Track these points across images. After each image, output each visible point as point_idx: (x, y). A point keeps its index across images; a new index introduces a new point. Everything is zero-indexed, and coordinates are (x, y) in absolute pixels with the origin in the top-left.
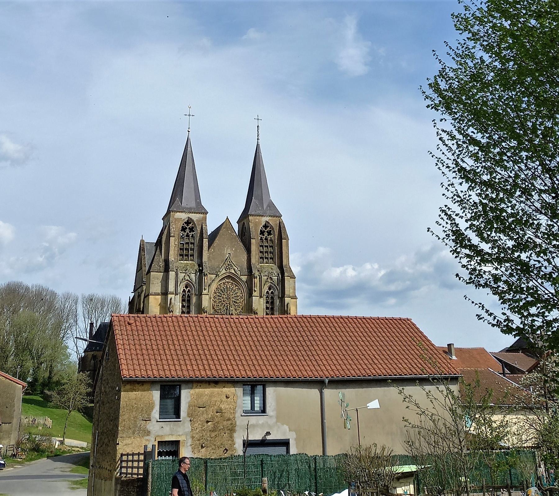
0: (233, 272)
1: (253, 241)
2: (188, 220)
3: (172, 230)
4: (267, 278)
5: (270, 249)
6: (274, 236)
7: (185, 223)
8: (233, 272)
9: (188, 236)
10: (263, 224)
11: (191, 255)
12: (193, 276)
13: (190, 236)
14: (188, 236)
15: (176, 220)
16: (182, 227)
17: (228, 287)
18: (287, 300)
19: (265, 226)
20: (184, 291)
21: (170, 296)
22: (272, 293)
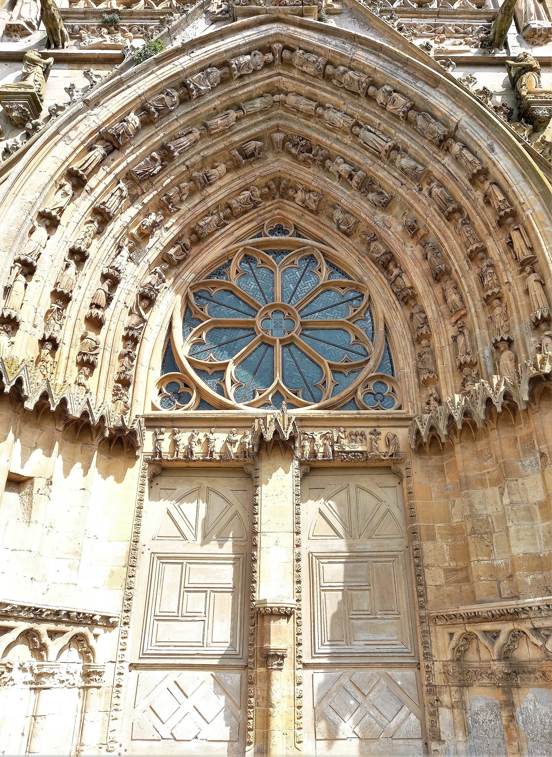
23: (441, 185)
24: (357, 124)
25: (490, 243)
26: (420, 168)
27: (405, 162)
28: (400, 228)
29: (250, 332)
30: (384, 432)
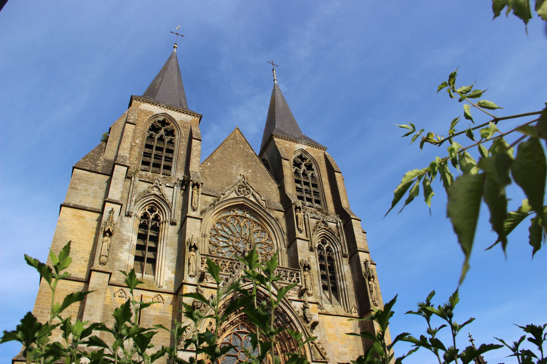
0: (252, 199)
1: (285, 162)
4: (317, 223)
7: (159, 122)
8: (252, 199)
15: (141, 111)
18: (363, 257)
19: (300, 157)
20: (145, 216)
22: (328, 249)
27: (280, 322)
29: (235, 358)
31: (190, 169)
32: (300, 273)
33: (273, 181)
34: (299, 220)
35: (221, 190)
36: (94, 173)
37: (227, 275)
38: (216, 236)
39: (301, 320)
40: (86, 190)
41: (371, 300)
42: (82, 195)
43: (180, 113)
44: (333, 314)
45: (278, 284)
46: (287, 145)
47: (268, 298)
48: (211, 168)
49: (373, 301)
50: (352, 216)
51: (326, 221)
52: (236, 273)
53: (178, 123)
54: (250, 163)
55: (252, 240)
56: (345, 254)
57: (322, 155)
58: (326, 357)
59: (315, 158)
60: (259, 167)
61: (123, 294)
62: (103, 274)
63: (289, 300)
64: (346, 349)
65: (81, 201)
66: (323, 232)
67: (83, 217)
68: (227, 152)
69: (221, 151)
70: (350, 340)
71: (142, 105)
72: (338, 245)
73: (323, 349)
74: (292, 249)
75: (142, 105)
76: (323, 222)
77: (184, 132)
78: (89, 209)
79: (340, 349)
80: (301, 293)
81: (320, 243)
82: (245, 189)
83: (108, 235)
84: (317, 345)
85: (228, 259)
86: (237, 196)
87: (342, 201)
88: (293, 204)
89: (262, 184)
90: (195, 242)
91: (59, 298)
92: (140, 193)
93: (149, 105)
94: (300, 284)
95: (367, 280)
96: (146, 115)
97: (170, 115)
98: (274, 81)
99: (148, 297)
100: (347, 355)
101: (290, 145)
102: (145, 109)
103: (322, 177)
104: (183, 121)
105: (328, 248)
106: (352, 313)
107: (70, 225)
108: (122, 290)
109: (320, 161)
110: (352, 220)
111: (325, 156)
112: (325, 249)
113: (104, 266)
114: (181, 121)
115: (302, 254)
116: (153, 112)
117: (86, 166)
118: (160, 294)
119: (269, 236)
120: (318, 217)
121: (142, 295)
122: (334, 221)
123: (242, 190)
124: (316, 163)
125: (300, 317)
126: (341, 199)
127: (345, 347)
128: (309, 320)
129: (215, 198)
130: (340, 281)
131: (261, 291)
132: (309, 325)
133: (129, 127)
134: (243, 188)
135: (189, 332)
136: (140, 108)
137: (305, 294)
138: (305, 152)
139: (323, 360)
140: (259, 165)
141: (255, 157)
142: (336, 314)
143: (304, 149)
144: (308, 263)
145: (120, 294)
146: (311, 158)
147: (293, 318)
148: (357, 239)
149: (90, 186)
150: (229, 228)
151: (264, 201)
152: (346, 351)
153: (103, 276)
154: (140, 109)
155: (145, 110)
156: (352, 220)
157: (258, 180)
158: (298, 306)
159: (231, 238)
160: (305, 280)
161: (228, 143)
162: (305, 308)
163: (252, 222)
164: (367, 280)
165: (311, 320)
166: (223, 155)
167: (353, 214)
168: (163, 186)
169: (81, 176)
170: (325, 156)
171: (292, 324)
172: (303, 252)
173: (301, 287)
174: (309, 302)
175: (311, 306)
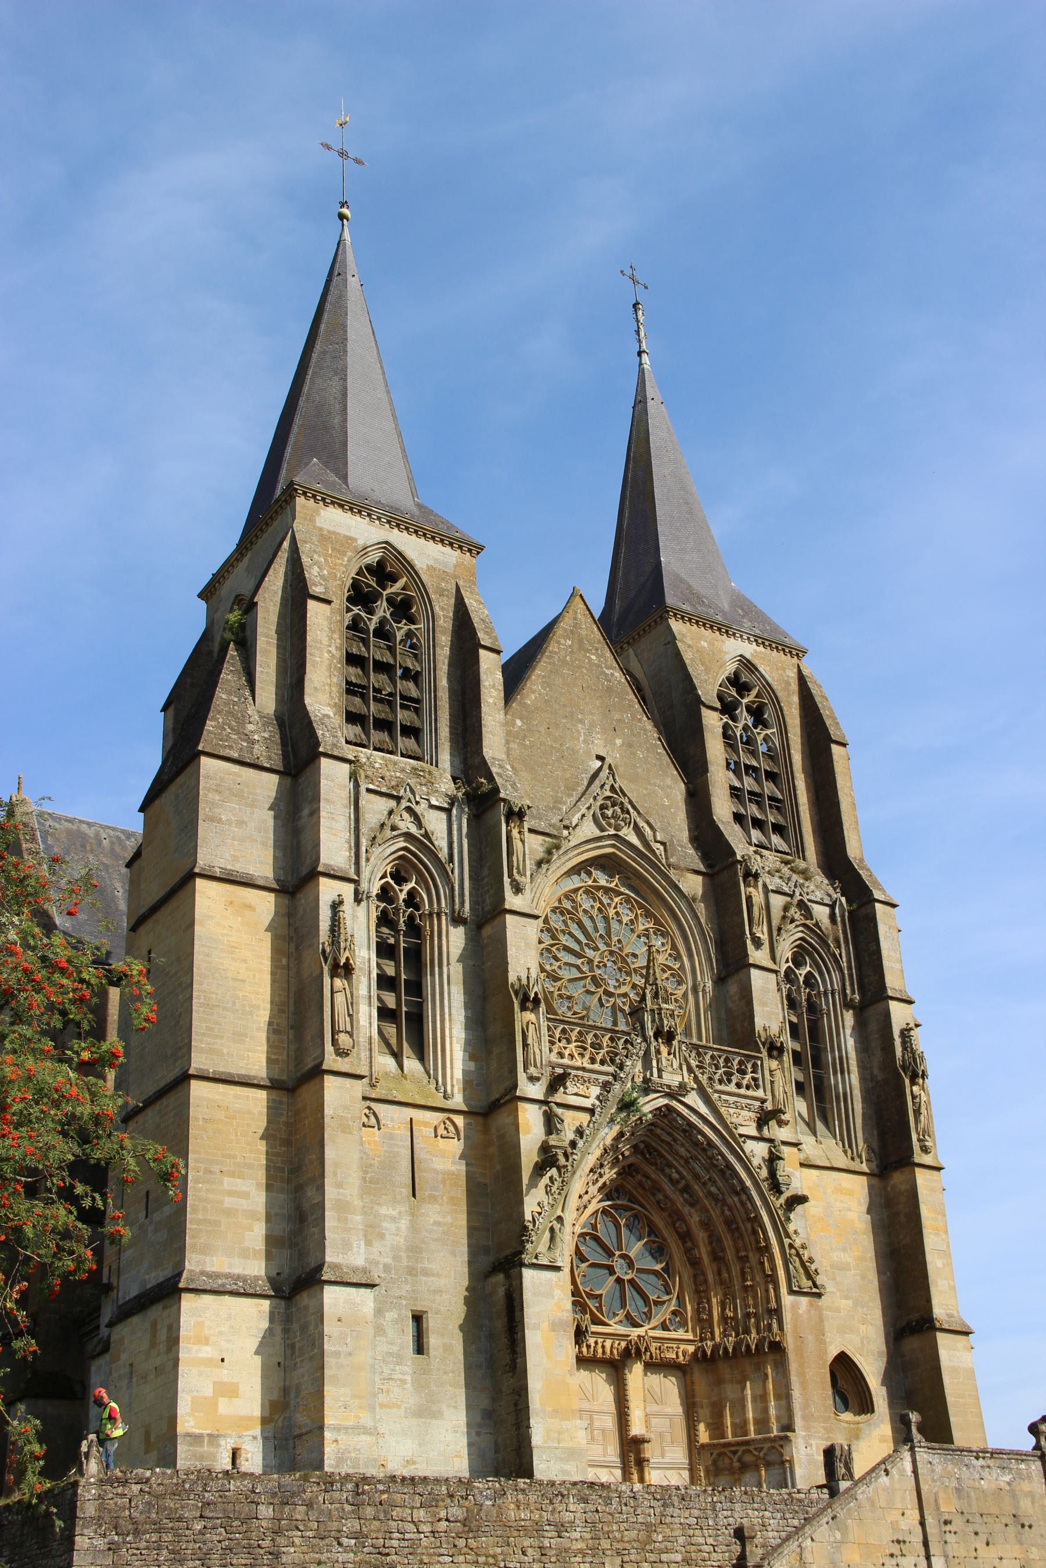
0: (634, 840)
2: (381, 564)
3: (312, 573)
4: (786, 908)
5: (769, 788)
6: (783, 730)
8: (634, 840)
9: (382, 632)
10: (730, 668)
11: (412, 731)
12: (436, 824)
13: (399, 635)
14: (382, 632)
15: (327, 538)
16: (355, 585)
17: (611, 912)
19: (735, 680)
21: (328, 890)
23: (730, 1209)
24: (691, 1158)
25: (751, 1254)
26: (720, 1196)
27: (713, 1189)
28: (697, 1219)
30: (682, 1347)
31: (484, 750)
32: (759, 1063)
33: (675, 773)
34: (756, 910)
35: (554, 807)
36: (251, 770)
37: (606, 1074)
38: (554, 949)
39: (765, 1186)
40: (241, 823)
41: (914, 1137)
42: (233, 839)
43: (422, 540)
44: (821, 1164)
45: (716, 1095)
46: (702, 643)
47: (695, 1132)
48: (525, 737)
49: (919, 1140)
50: (877, 895)
51: (809, 901)
52: (627, 1069)
53: (424, 578)
54: (617, 716)
55: (658, 976)
56: (852, 1000)
57: (793, 674)
58: (819, 1280)
59: (775, 687)
60: (641, 729)
61: (373, 1118)
62: (348, 1082)
63: (741, 1136)
64: (846, 1255)
65: (235, 858)
66: (800, 935)
67: (250, 907)
68: (559, 681)
69: (544, 677)
70: (856, 1232)
71: (322, 512)
72: (834, 971)
73: (811, 1260)
74: (733, 988)
75: (322, 512)
76: (801, 905)
77: (443, 609)
78: (261, 882)
79: (835, 1254)
80: (764, 1119)
81: (790, 964)
82: (617, 808)
83: (343, 974)
84: (801, 1251)
85: (605, 1029)
86: (597, 833)
87: (846, 839)
88: (739, 862)
89: (650, 784)
90: (536, 989)
91: (236, 1135)
92: (372, 829)
93: (340, 511)
94: (760, 1093)
95: (907, 1082)
96: (338, 551)
97: (401, 547)
98: (640, 354)
99: (426, 1124)
100: (850, 1270)
101: (711, 644)
102: (332, 529)
103: (792, 752)
104: (435, 569)
105: (809, 976)
106: (862, 1163)
107: (225, 932)
108: (369, 1108)
109: (789, 695)
110: (877, 905)
111: (802, 679)
112: (801, 979)
113: (346, 1059)
114: (430, 568)
115: (763, 1011)
116: (355, 540)
117: (230, 747)
118: (452, 1116)
119: (674, 947)
120: (786, 889)
121: (411, 1119)
122: (827, 901)
123: (609, 813)
124: (776, 700)
125: (764, 1181)
126: (845, 832)
127: (844, 1250)
128: (783, 1189)
129: (547, 839)
130: (835, 1073)
131: (679, 1114)
132: (782, 1200)
133: (316, 613)
134: (613, 806)
135: (541, 1220)
136: (318, 524)
137: (773, 1123)
138: (747, 664)
139: (814, 1290)
140: (640, 720)
141: (627, 694)
142: (829, 1165)
143: (748, 656)
144: (782, 1039)
145: (365, 1119)
146: (764, 686)
147: (748, 1183)
148: (886, 963)
149: (249, 810)
150: (581, 925)
151: (663, 844)
152: (849, 1260)
153: (348, 1086)
154: (321, 529)
155: (334, 533)
156: (877, 905)
157: (640, 770)
158: (757, 1151)
159: (590, 953)
160: (772, 1082)
161: (559, 648)
162: (773, 1159)
163: (633, 906)
164: (907, 1082)
165: (788, 1189)
166: (551, 690)
167: (882, 890)
168: (424, 805)
169: (222, 779)
170: (802, 679)
171: (744, 1197)
172: (765, 1004)
173: (763, 1101)
174: (784, 1143)
175: (786, 1150)
